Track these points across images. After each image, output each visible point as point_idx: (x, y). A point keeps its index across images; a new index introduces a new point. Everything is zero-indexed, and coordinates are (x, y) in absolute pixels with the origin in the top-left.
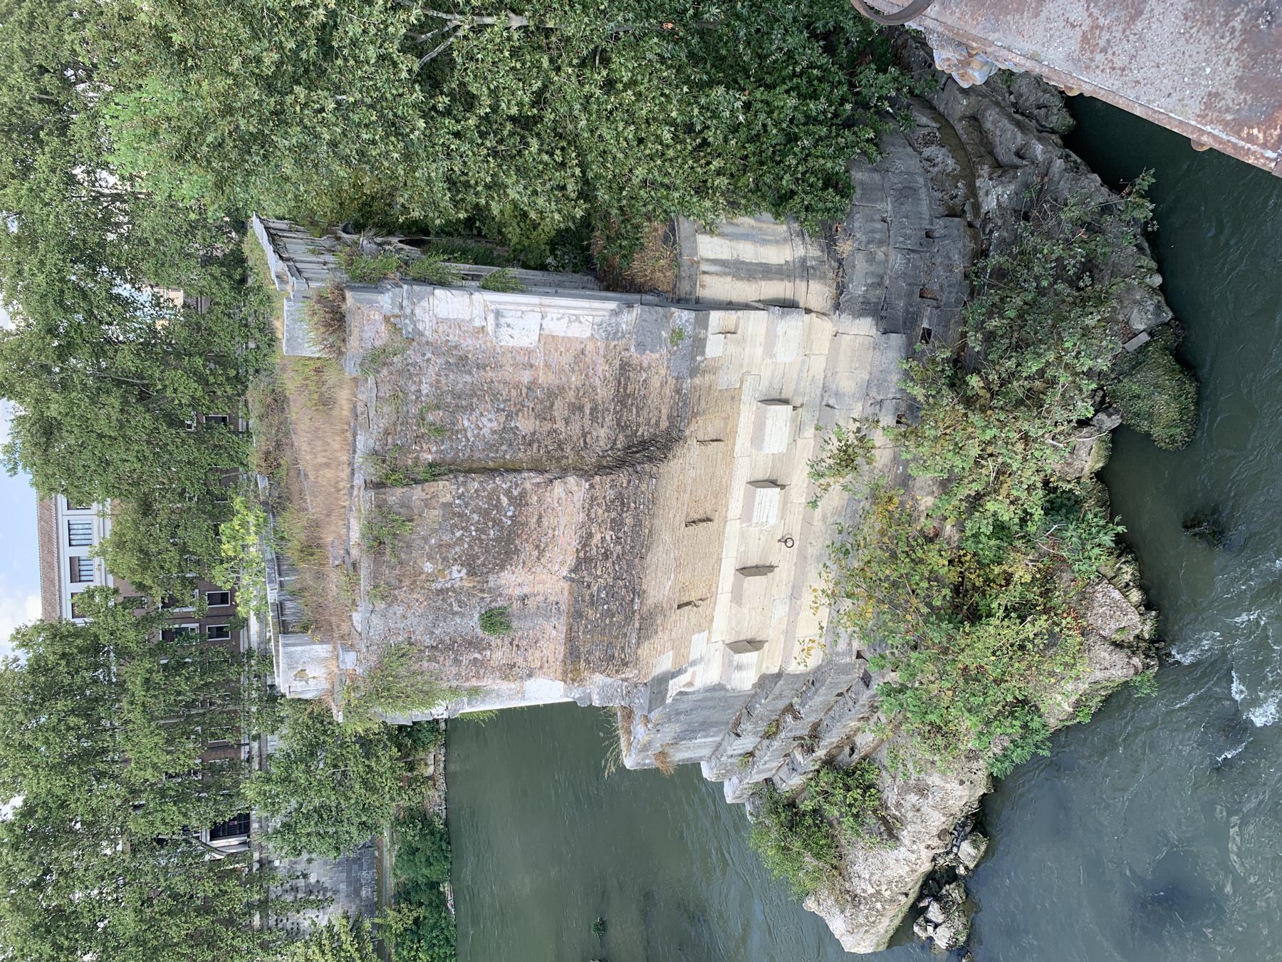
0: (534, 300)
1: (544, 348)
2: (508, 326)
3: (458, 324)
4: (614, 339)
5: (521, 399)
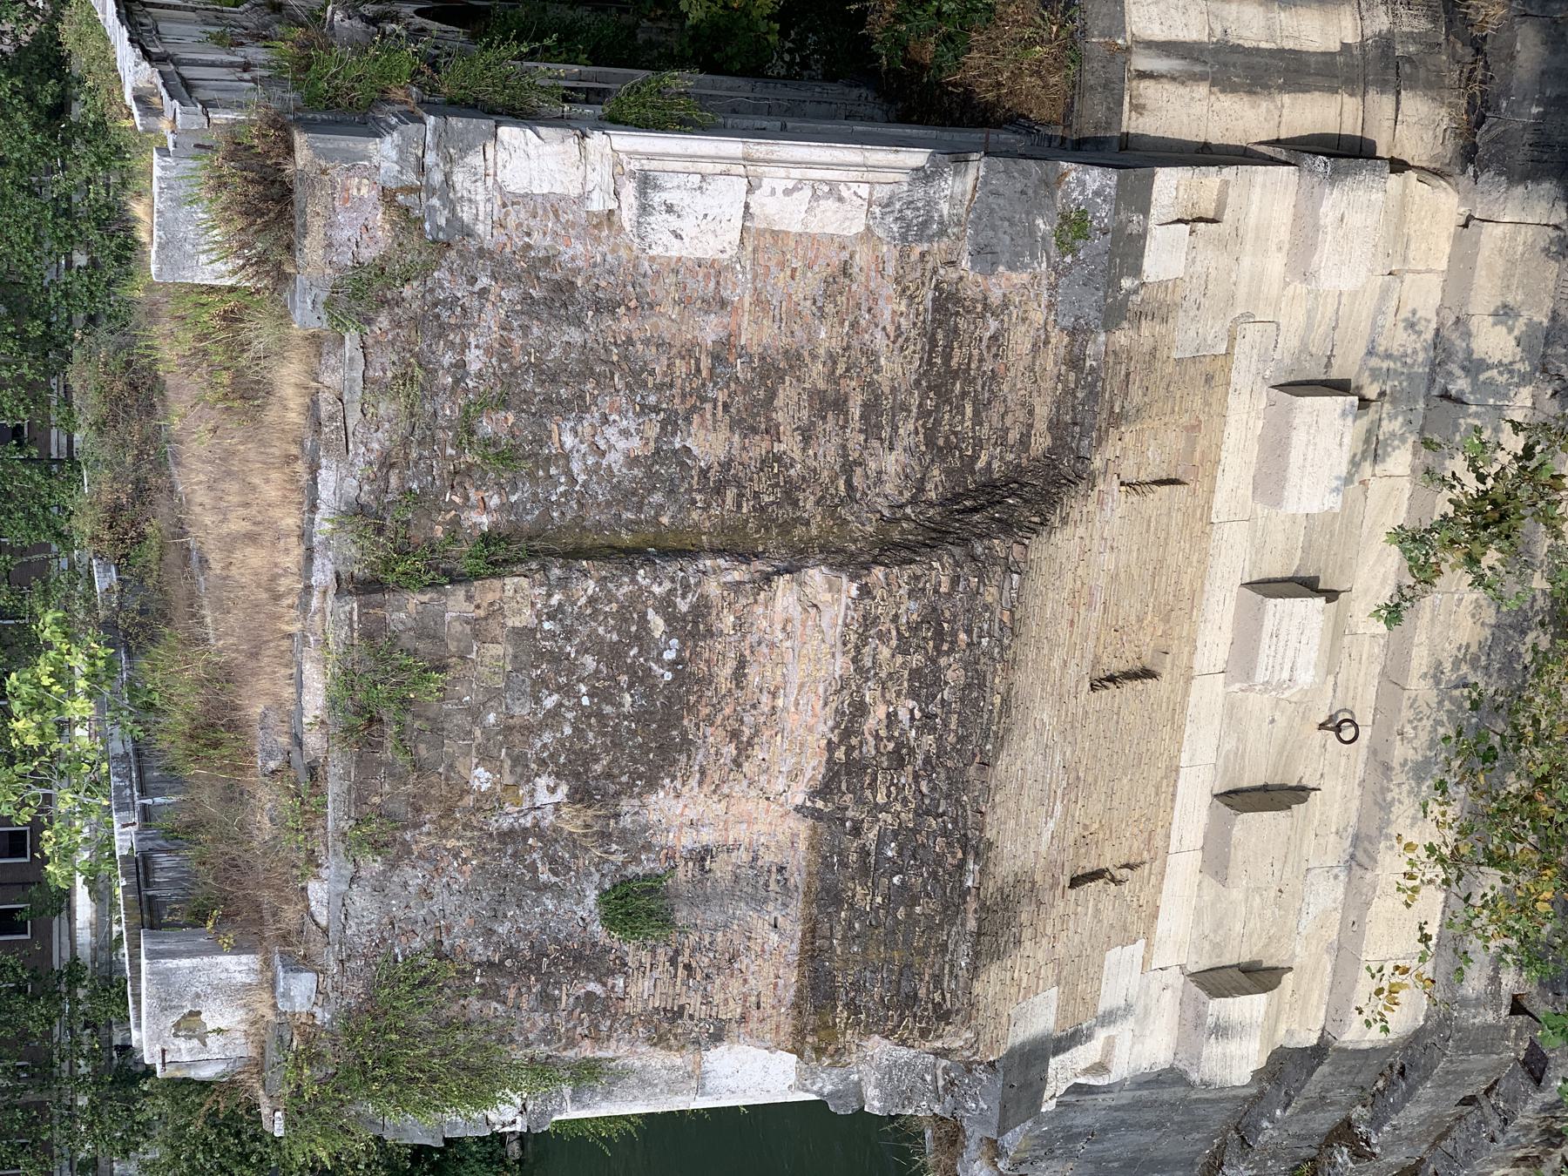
0: (732, 147)
1: (754, 261)
2: (670, 209)
3: (553, 206)
4: (920, 238)
5: (697, 383)
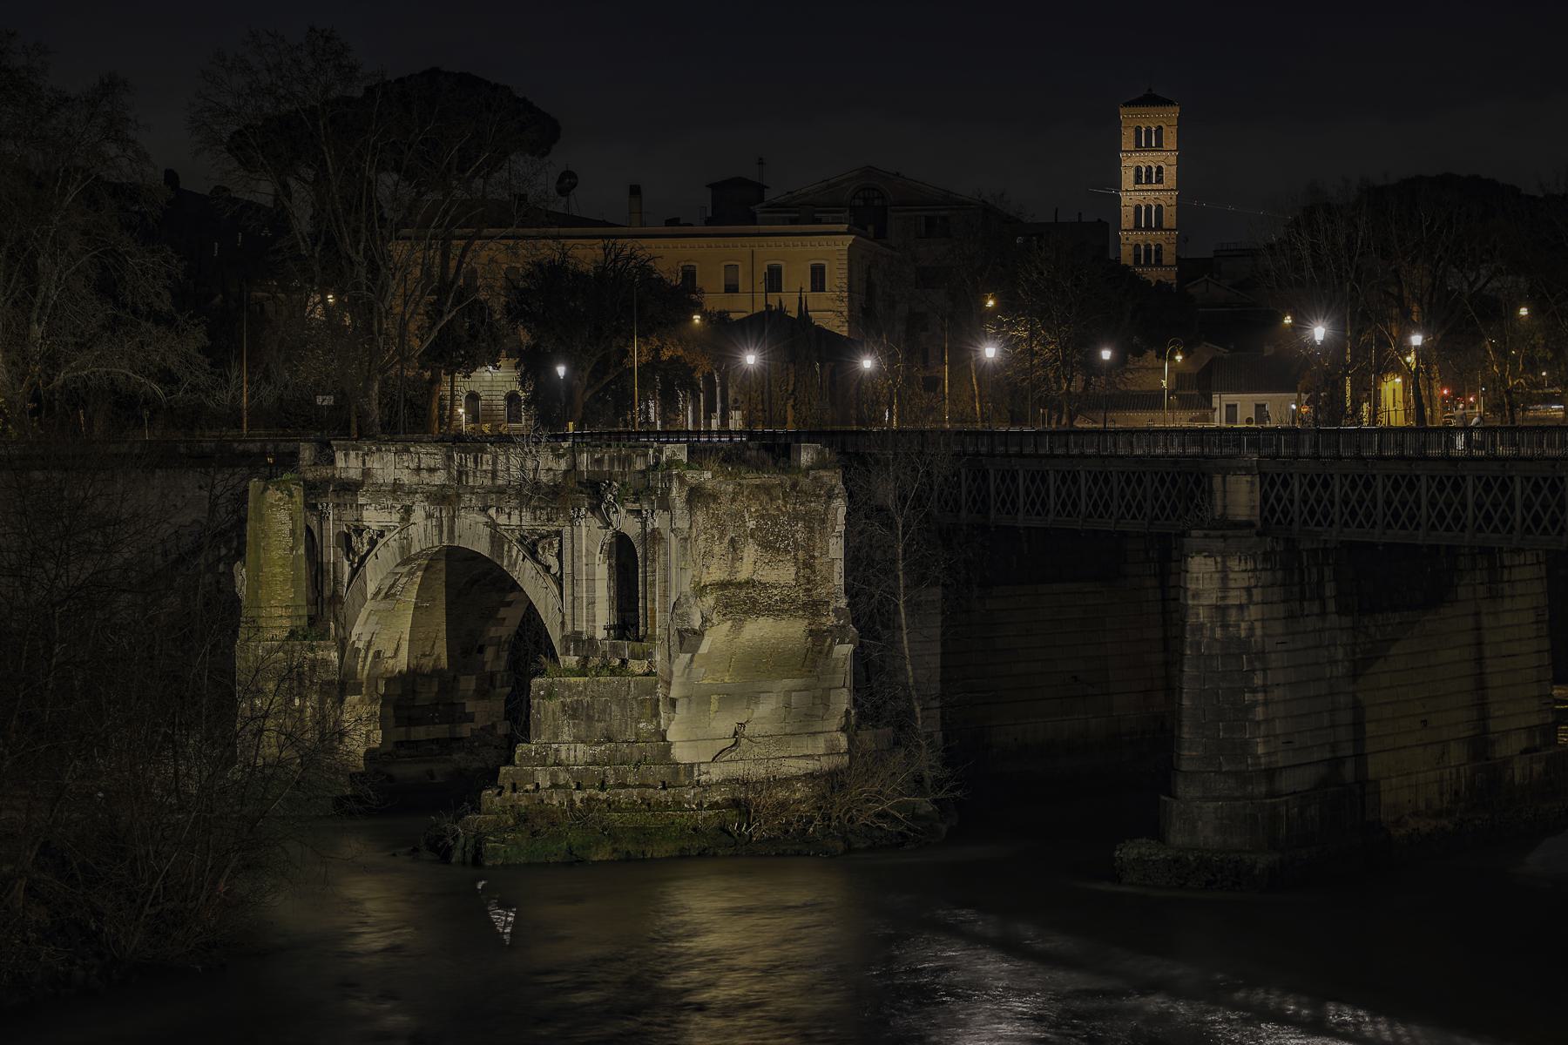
3: (836, 519)
